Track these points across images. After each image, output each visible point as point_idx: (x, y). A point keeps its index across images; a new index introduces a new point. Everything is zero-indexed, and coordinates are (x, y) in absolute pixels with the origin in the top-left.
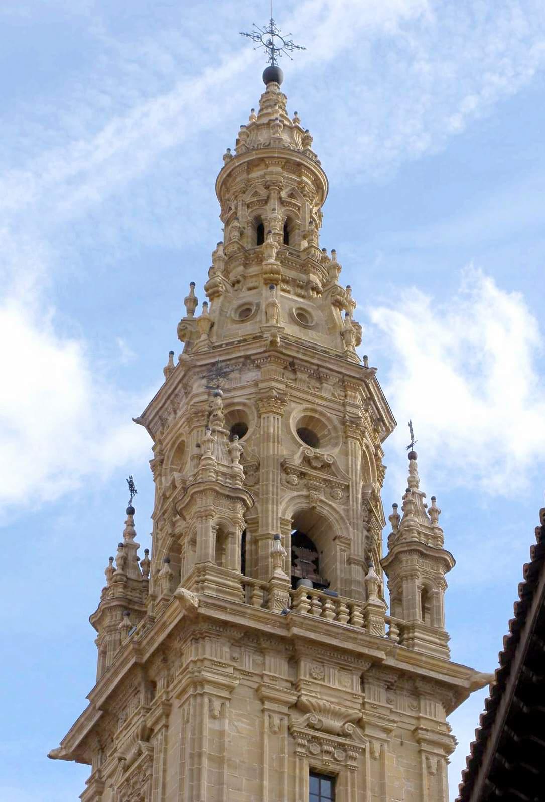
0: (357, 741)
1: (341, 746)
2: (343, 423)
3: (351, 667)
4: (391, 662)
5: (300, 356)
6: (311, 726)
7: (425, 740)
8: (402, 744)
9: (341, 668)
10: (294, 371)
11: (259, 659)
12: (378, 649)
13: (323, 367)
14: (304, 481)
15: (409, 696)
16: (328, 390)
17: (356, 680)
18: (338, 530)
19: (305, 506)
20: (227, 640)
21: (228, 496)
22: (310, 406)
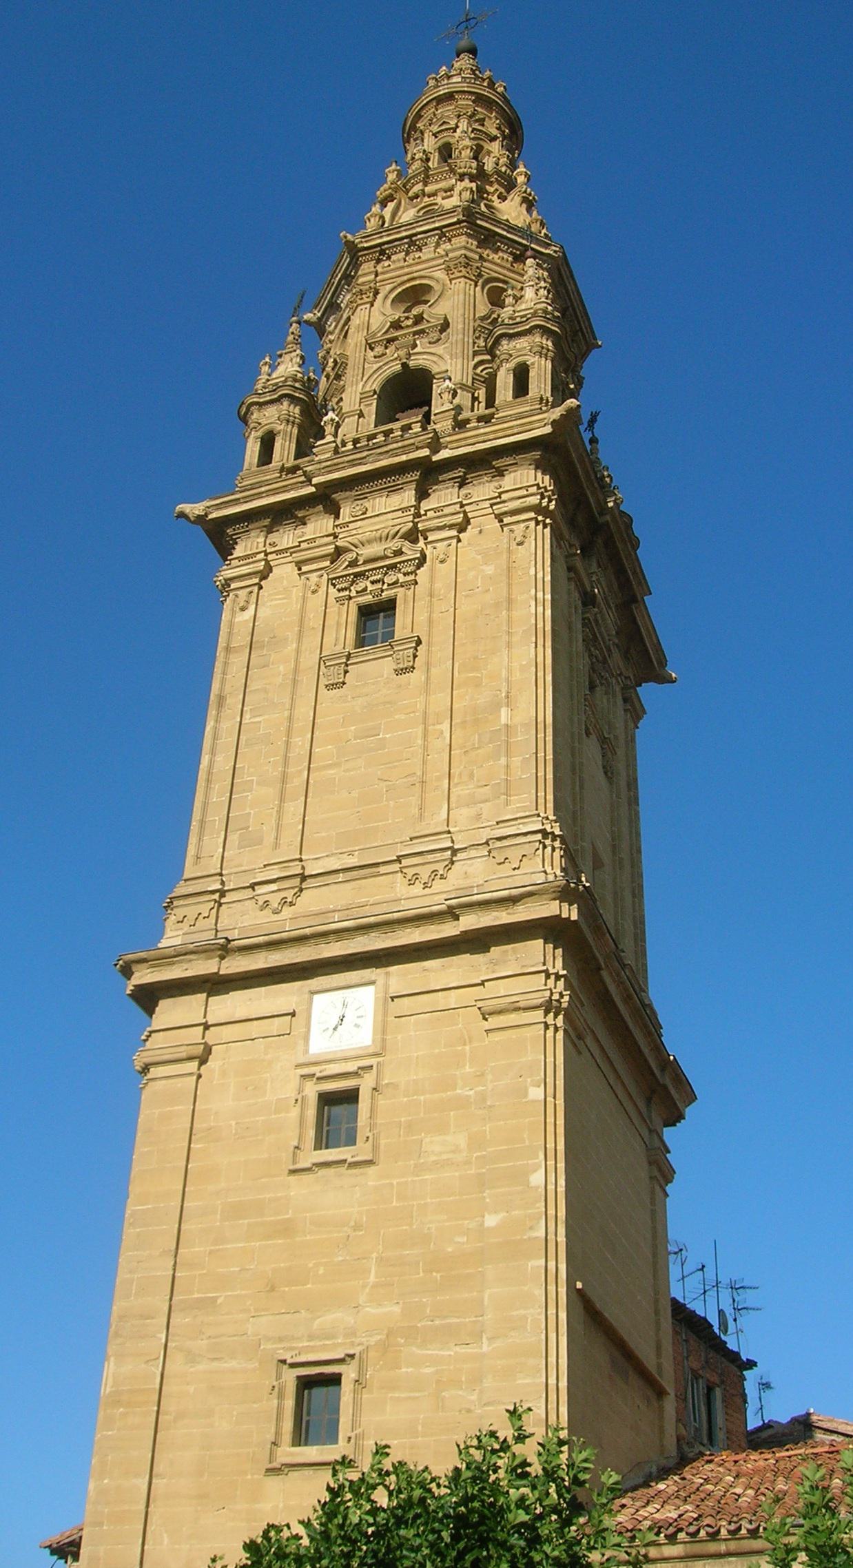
0: (409, 553)
1: (393, 567)
2: (448, 269)
3: (399, 485)
4: (444, 454)
5: (385, 239)
6: (353, 564)
7: (505, 513)
8: (480, 532)
9: (389, 492)
10: (389, 258)
11: (299, 531)
12: (418, 448)
13: (415, 235)
14: (392, 348)
15: (491, 481)
16: (427, 253)
17: (408, 497)
18: (435, 369)
19: (397, 367)
20: (259, 530)
21: (272, 402)
22: (405, 278)
